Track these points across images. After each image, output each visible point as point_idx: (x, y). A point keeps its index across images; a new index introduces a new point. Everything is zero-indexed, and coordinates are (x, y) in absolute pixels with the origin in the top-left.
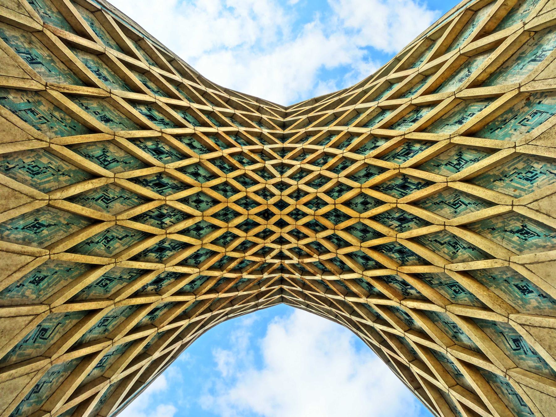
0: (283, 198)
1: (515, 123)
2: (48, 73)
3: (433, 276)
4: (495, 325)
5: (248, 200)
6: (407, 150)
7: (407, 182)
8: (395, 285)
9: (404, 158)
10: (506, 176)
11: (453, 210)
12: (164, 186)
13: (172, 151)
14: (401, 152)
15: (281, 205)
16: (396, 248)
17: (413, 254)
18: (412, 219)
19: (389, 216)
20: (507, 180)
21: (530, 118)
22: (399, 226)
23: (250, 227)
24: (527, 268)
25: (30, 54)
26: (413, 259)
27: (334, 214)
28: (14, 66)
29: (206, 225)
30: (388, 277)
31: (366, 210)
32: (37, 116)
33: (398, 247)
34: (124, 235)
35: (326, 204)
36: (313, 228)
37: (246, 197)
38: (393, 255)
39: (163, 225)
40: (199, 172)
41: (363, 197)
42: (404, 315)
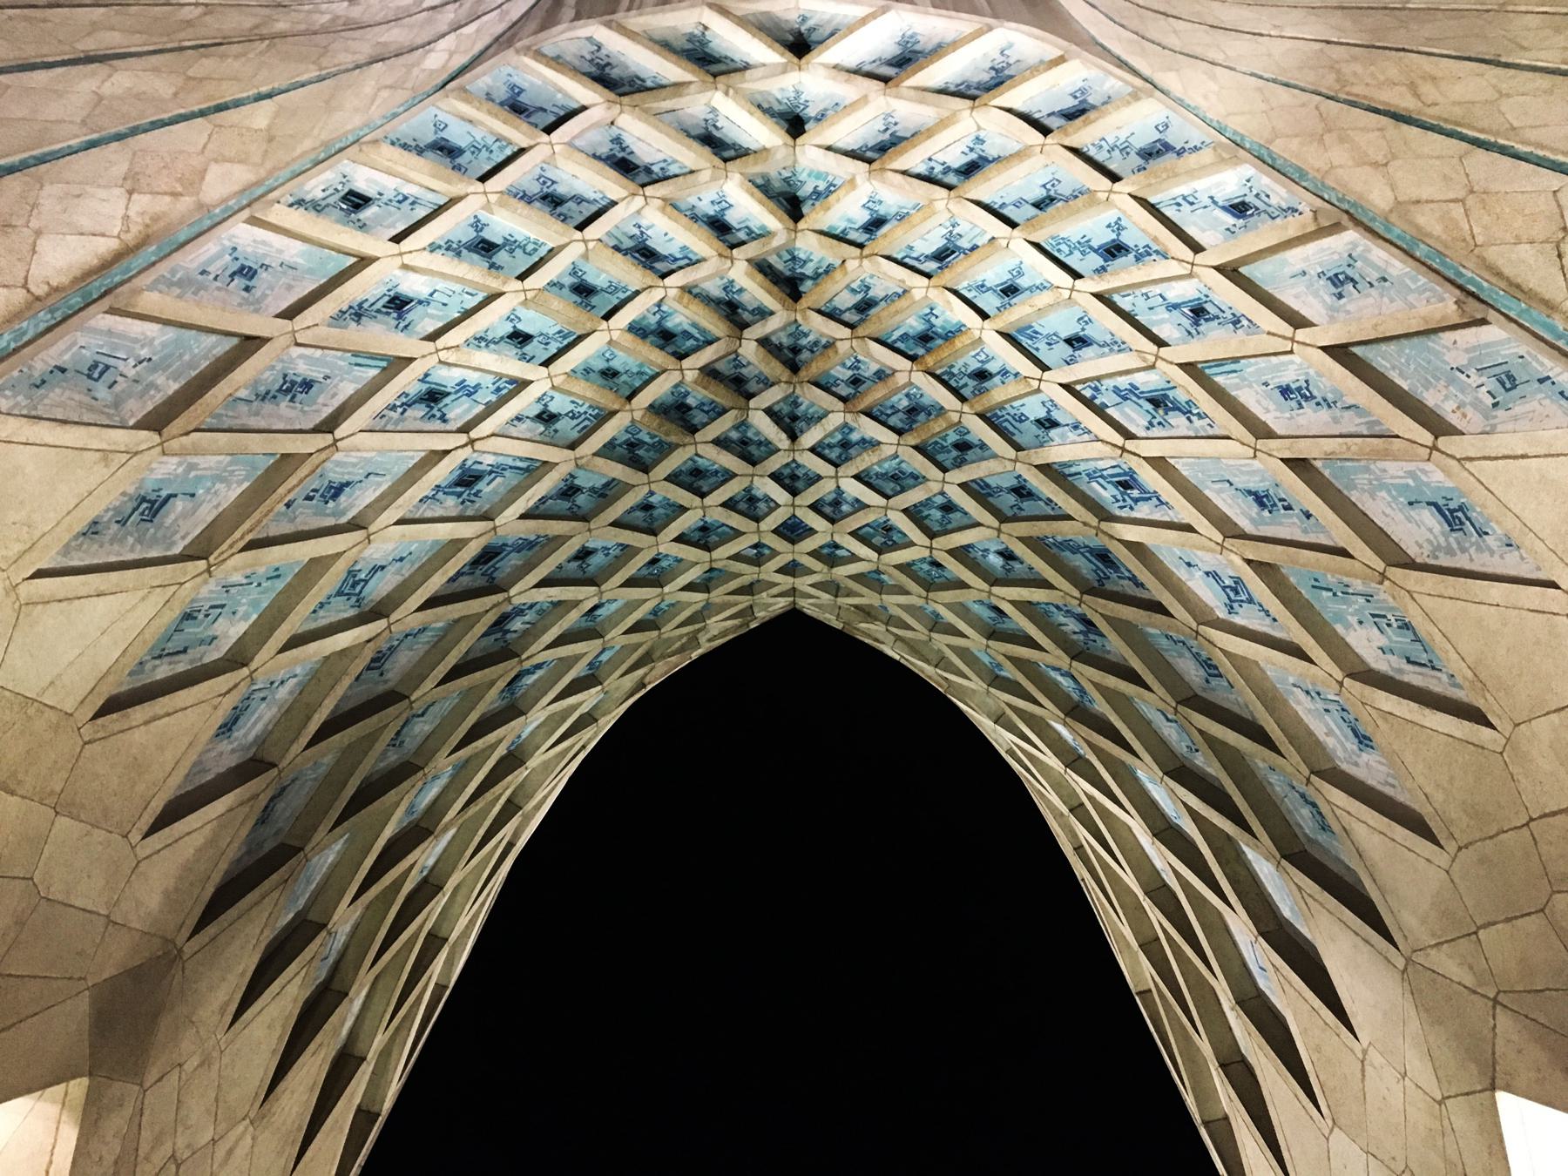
0: (799, 513)
1: (1364, 608)
2: (189, 504)
6: (1125, 474)
9: (1115, 492)
12: (497, 554)
13: (501, 460)
14: (1111, 471)
15: (793, 531)
20: (1320, 705)
21: (1395, 625)
25: (144, 499)
28: (143, 599)
32: (201, 616)
39: (508, 636)
40: (577, 482)
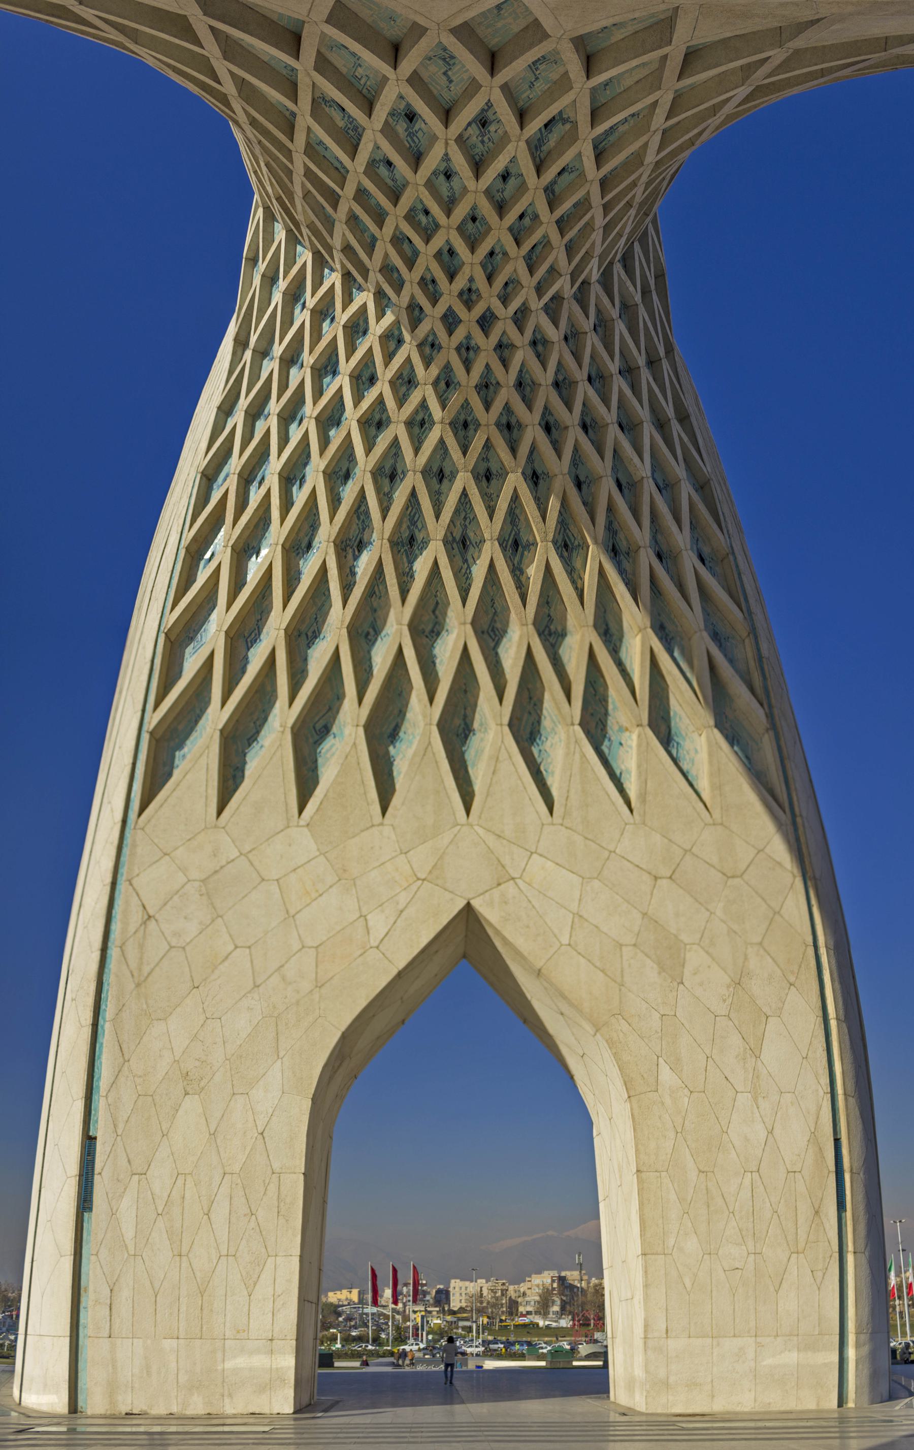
3: (382, 598)
4: (338, 699)
5: (500, 256)
6: (572, 544)
7: (524, 548)
8: (355, 526)
9: (560, 541)
10: (535, 705)
11: (485, 627)
14: (570, 534)
15: (486, 322)
16: (416, 531)
17: (411, 563)
18: (465, 561)
19: (468, 520)
22: (454, 539)
23: (446, 257)
24: (426, 748)
26: (403, 563)
27: (469, 419)
29: (455, 188)
30: (367, 513)
31: (476, 478)
33: (420, 536)
34: (453, 78)
35: (487, 406)
36: (443, 376)
37: (505, 254)
38: (404, 526)
41: (500, 471)
42: (307, 539)
